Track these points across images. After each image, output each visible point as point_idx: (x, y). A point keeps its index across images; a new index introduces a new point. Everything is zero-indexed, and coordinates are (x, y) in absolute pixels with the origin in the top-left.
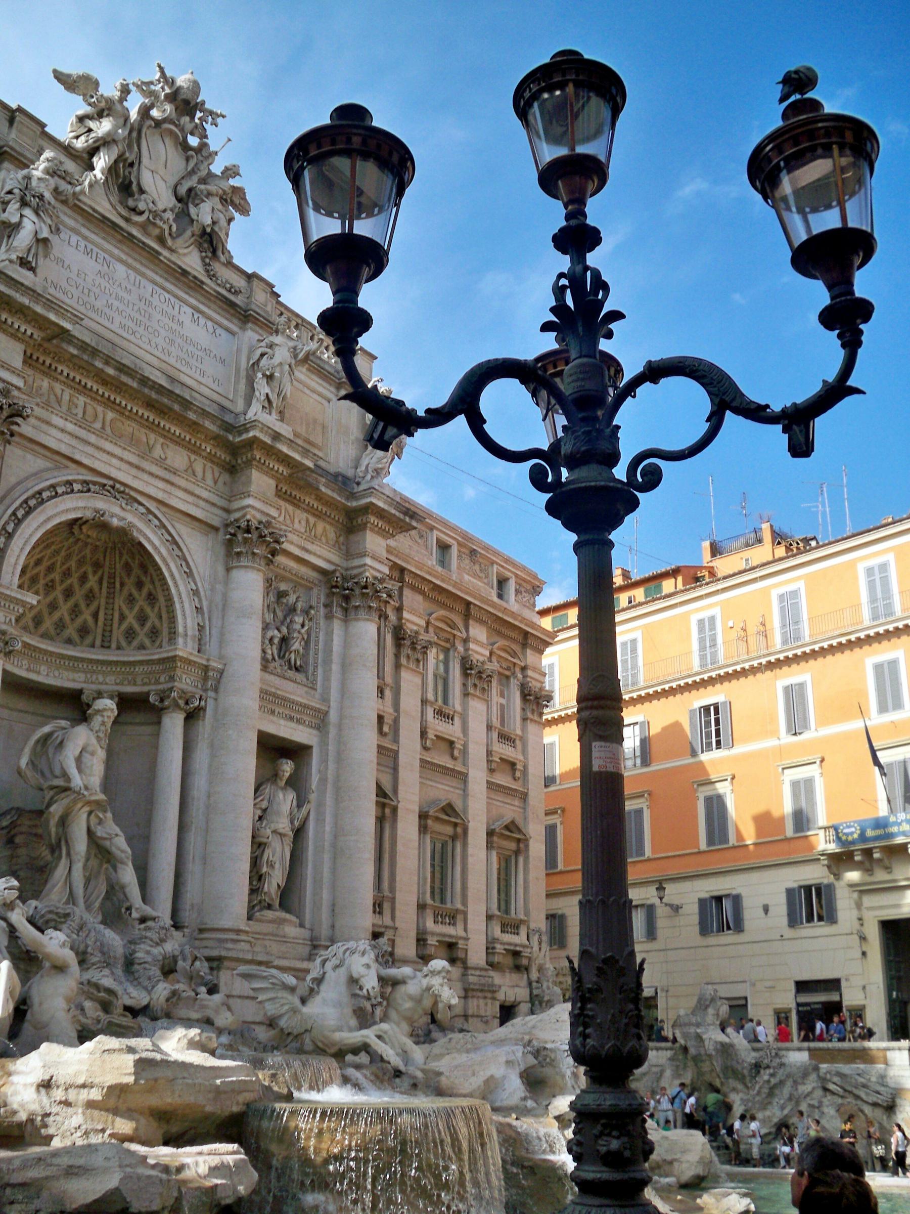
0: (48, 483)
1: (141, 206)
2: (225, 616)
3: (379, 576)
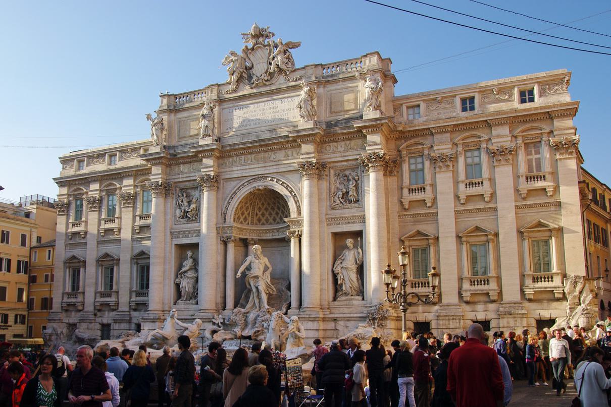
0: (237, 187)
1: (252, 82)
2: (304, 199)
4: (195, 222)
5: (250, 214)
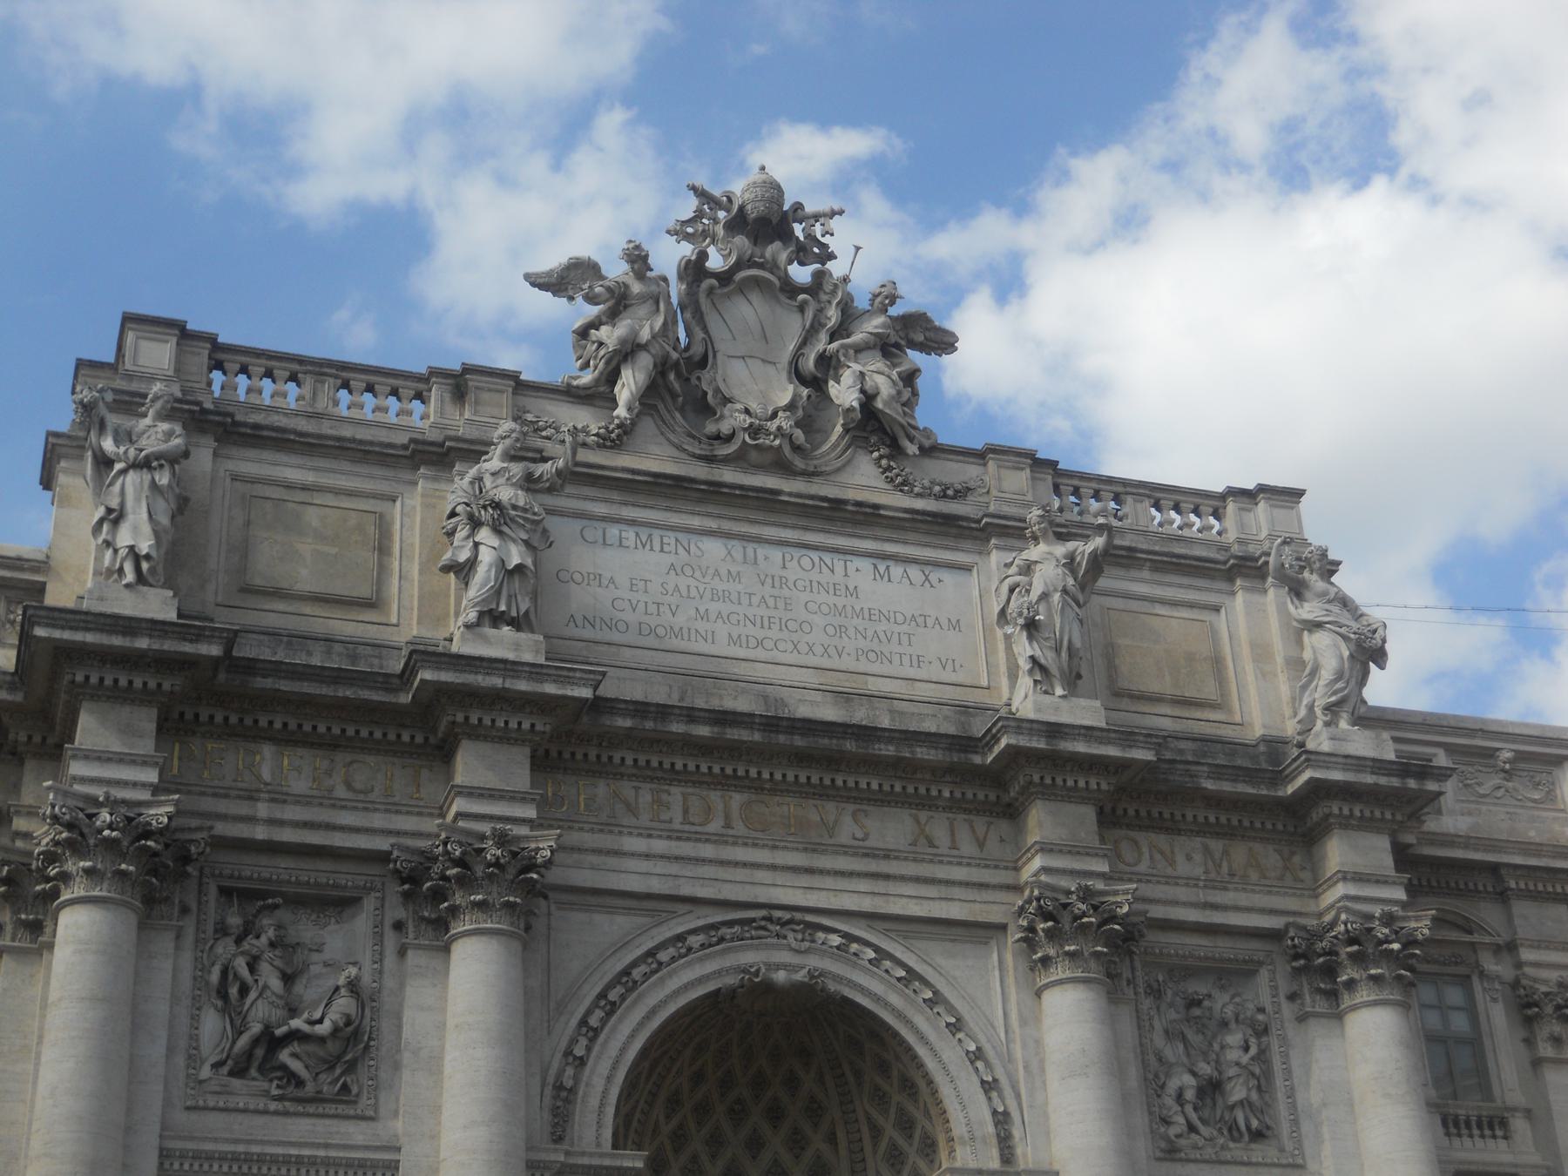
0: (639, 952)
1: (725, 428)
3: (1377, 910)
4: (341, 1109)
5: (637, 1115)
